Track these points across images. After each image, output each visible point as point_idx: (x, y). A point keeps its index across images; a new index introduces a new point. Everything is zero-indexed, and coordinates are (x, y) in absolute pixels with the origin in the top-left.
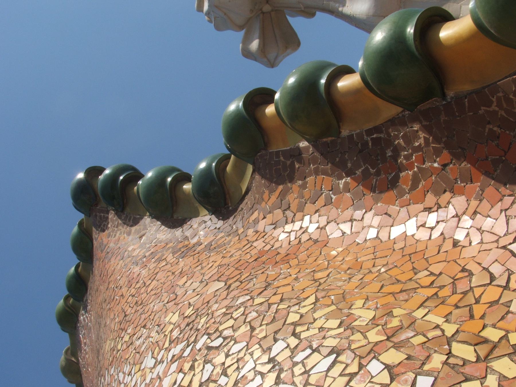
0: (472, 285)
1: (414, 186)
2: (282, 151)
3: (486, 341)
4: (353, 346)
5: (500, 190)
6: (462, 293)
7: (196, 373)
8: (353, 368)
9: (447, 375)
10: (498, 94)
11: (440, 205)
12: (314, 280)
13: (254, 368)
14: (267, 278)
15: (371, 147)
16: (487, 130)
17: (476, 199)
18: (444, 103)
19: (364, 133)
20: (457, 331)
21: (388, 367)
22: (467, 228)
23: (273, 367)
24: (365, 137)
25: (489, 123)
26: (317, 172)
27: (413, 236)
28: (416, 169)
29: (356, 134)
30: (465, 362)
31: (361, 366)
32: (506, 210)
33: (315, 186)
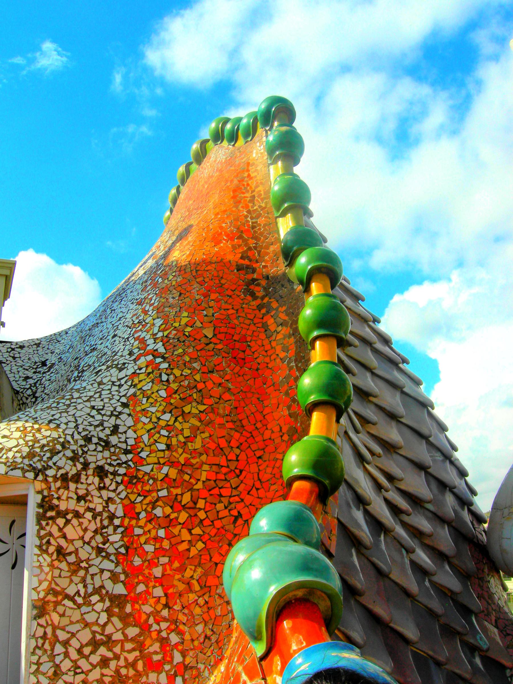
0: (231, 481)
3: (195, 503)
4: (174, 454)
6: (226, 478)
7: (146, 380)
8: (162, 461)
9: (171, 500)
12: (220, 396)
13: (153, 413)
14: (218, 365)
20: (198, 490)
21: (167, 475)
23: (156, 423)
26: (296, 342)
27: (267, 429)
30: (181, 501)
31: (164, 464)
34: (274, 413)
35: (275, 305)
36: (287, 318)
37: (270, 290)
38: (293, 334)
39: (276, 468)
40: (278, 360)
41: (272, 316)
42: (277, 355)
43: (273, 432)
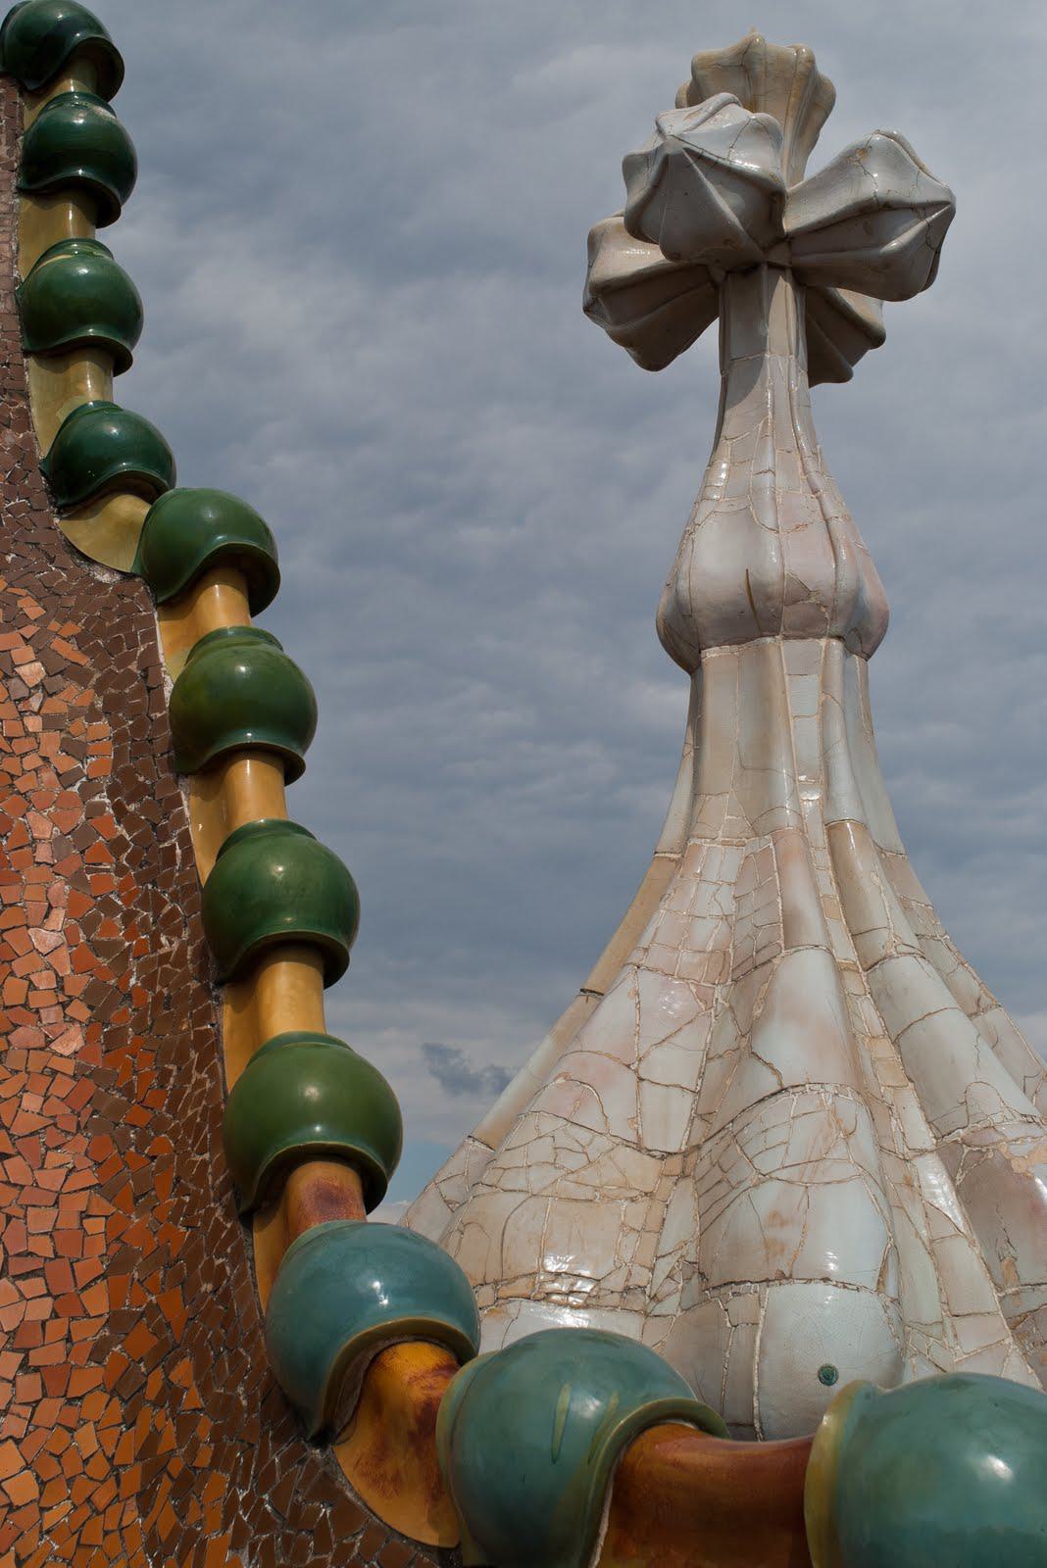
1: (98, 948)
2: (155, 646)
5: (89, 1105)
10: (208, 1080)
11: (68, 1005)
15: (161, 846)
16: (171, 1067)
17: (77, 1067)
18: (211, 985)
19: (183, 828)
22: (26, 1068)
24: (178, 831)
25: (179, 1069)
26: (118, 738)
27: (12, 974)
28: (127, 944)
29: (182, 811)
32: (55, 1125)
33: (93, 741)
34: (31, 931)
35: (33, 610)
36: (85, 661)
37: (9, 559)
38: (106, 712)
39: (53, 1099)
40: (48, 776)
41: (26, 640)
42: (45, 759)
43: (32, 986)
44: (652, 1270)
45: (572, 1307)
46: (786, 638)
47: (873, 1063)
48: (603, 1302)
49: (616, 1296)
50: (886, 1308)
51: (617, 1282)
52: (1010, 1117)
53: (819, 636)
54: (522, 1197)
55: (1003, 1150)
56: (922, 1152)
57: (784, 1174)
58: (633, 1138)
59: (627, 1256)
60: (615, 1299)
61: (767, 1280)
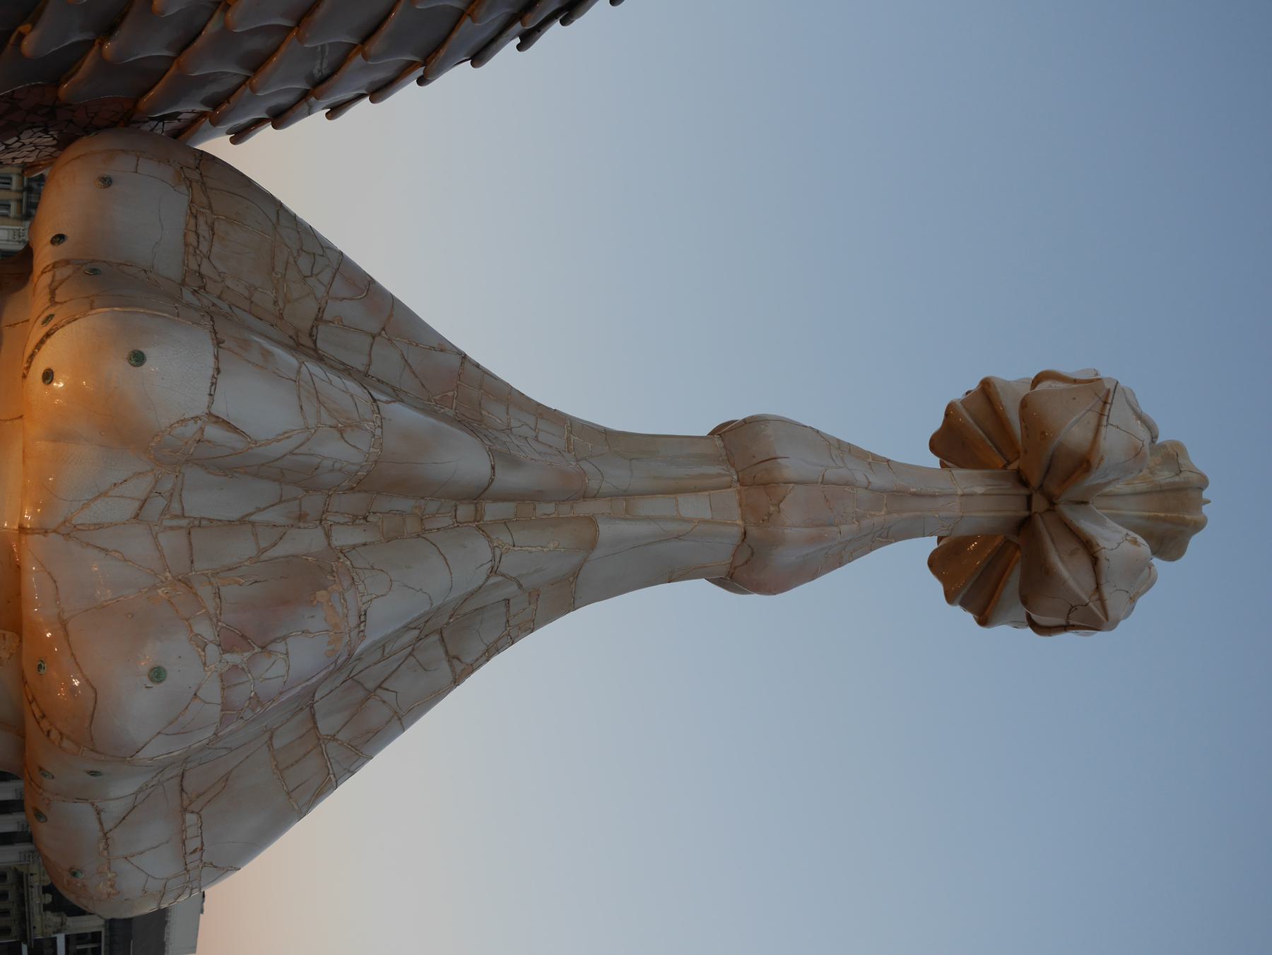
44: (219, 297)
45: (185, 235)
46: (739, 492)
47: (402, 513)
48: (190, 257)
49: (196, 268)
50: (196, 419)
51: (206, 269)
52: (364, 599)
53: (743, 519)
54: (274, 220)
55: (335, 587)
56: (328, 536)
57: (304, 369)
58: (327, 316)
59: (229, 283)
60: (194, 267)
61: (216, 333)
